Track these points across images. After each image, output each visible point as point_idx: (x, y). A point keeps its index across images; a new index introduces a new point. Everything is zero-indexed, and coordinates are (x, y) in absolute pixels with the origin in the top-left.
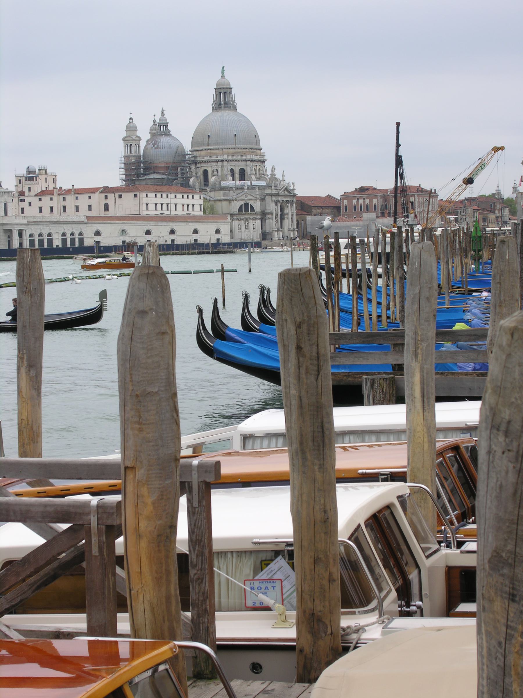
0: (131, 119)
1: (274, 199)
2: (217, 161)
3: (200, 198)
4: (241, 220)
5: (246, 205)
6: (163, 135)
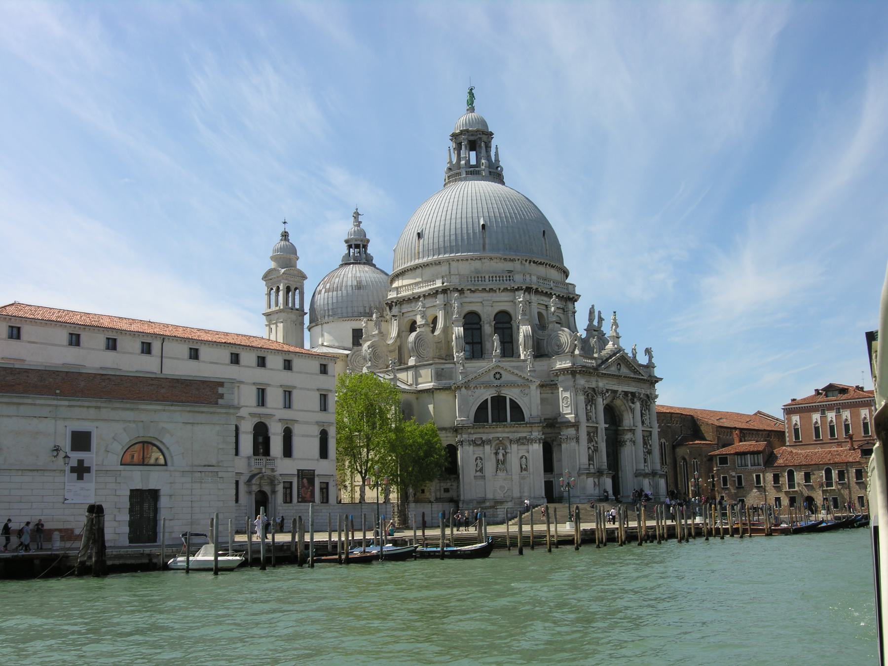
0: (285, 236)
1: (582, 381)
2: (435, 293)
3: (324, 370)
4: (483, 443)
5: (498, 401)
6: (350, 264)
